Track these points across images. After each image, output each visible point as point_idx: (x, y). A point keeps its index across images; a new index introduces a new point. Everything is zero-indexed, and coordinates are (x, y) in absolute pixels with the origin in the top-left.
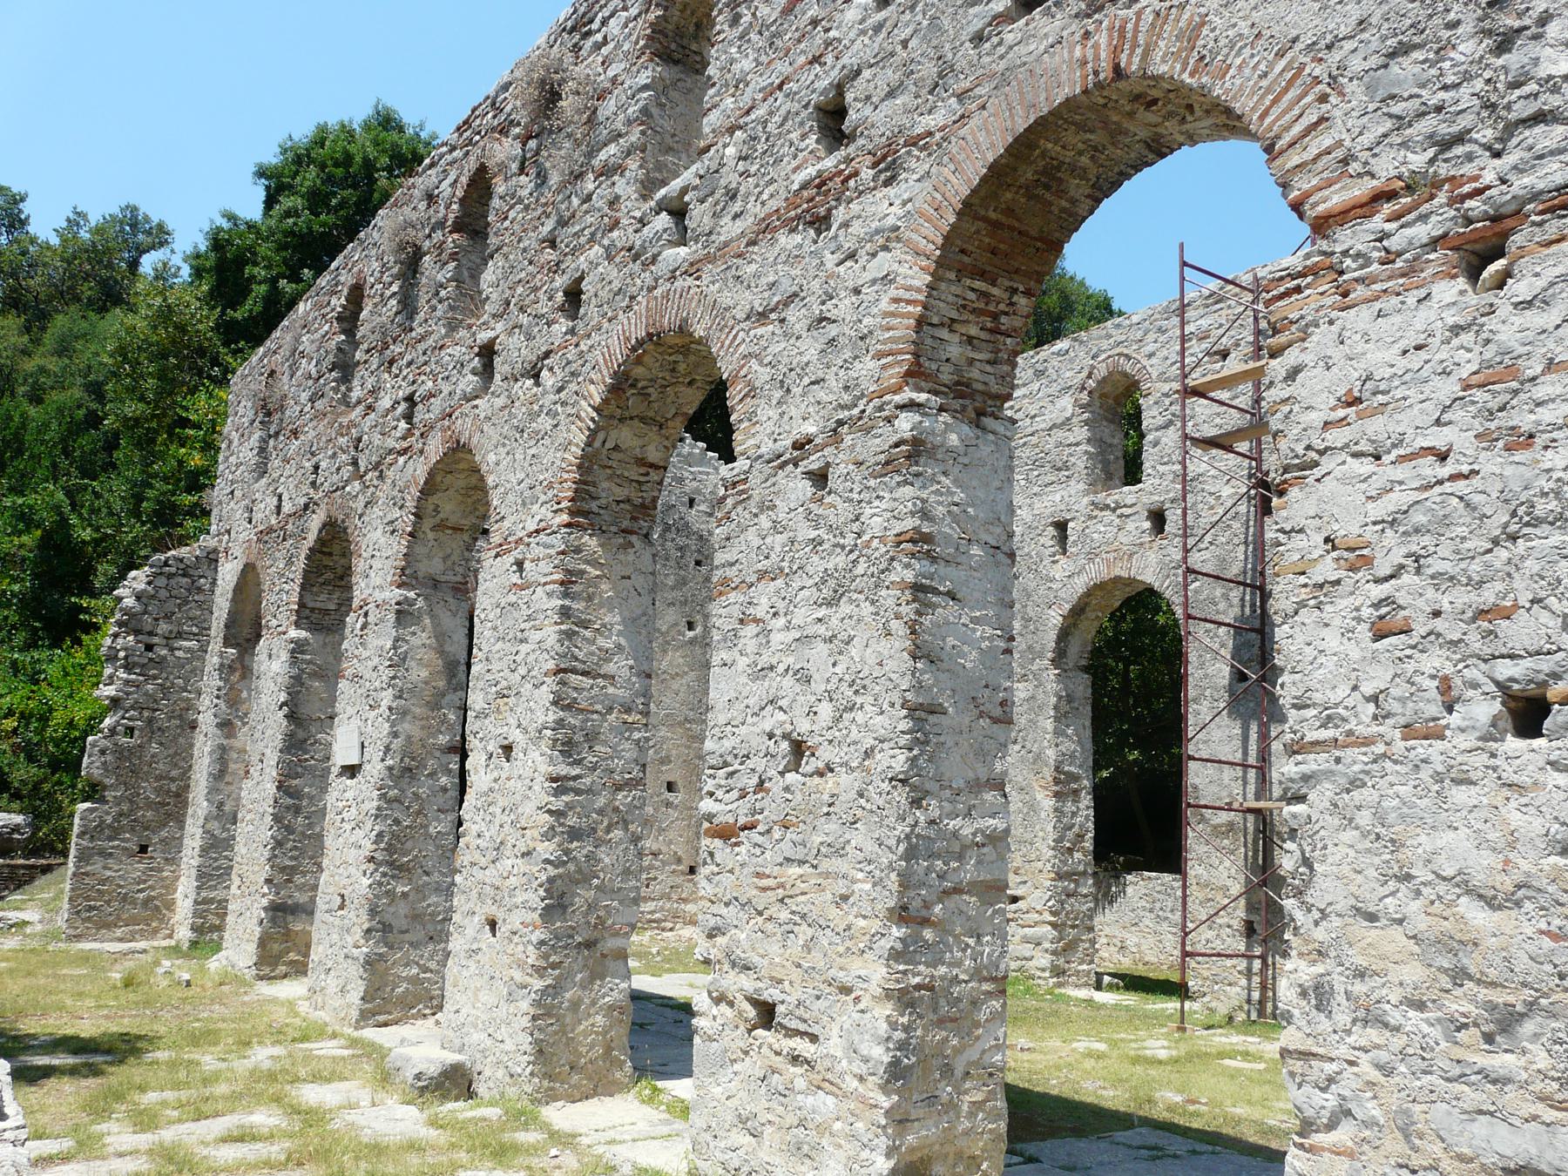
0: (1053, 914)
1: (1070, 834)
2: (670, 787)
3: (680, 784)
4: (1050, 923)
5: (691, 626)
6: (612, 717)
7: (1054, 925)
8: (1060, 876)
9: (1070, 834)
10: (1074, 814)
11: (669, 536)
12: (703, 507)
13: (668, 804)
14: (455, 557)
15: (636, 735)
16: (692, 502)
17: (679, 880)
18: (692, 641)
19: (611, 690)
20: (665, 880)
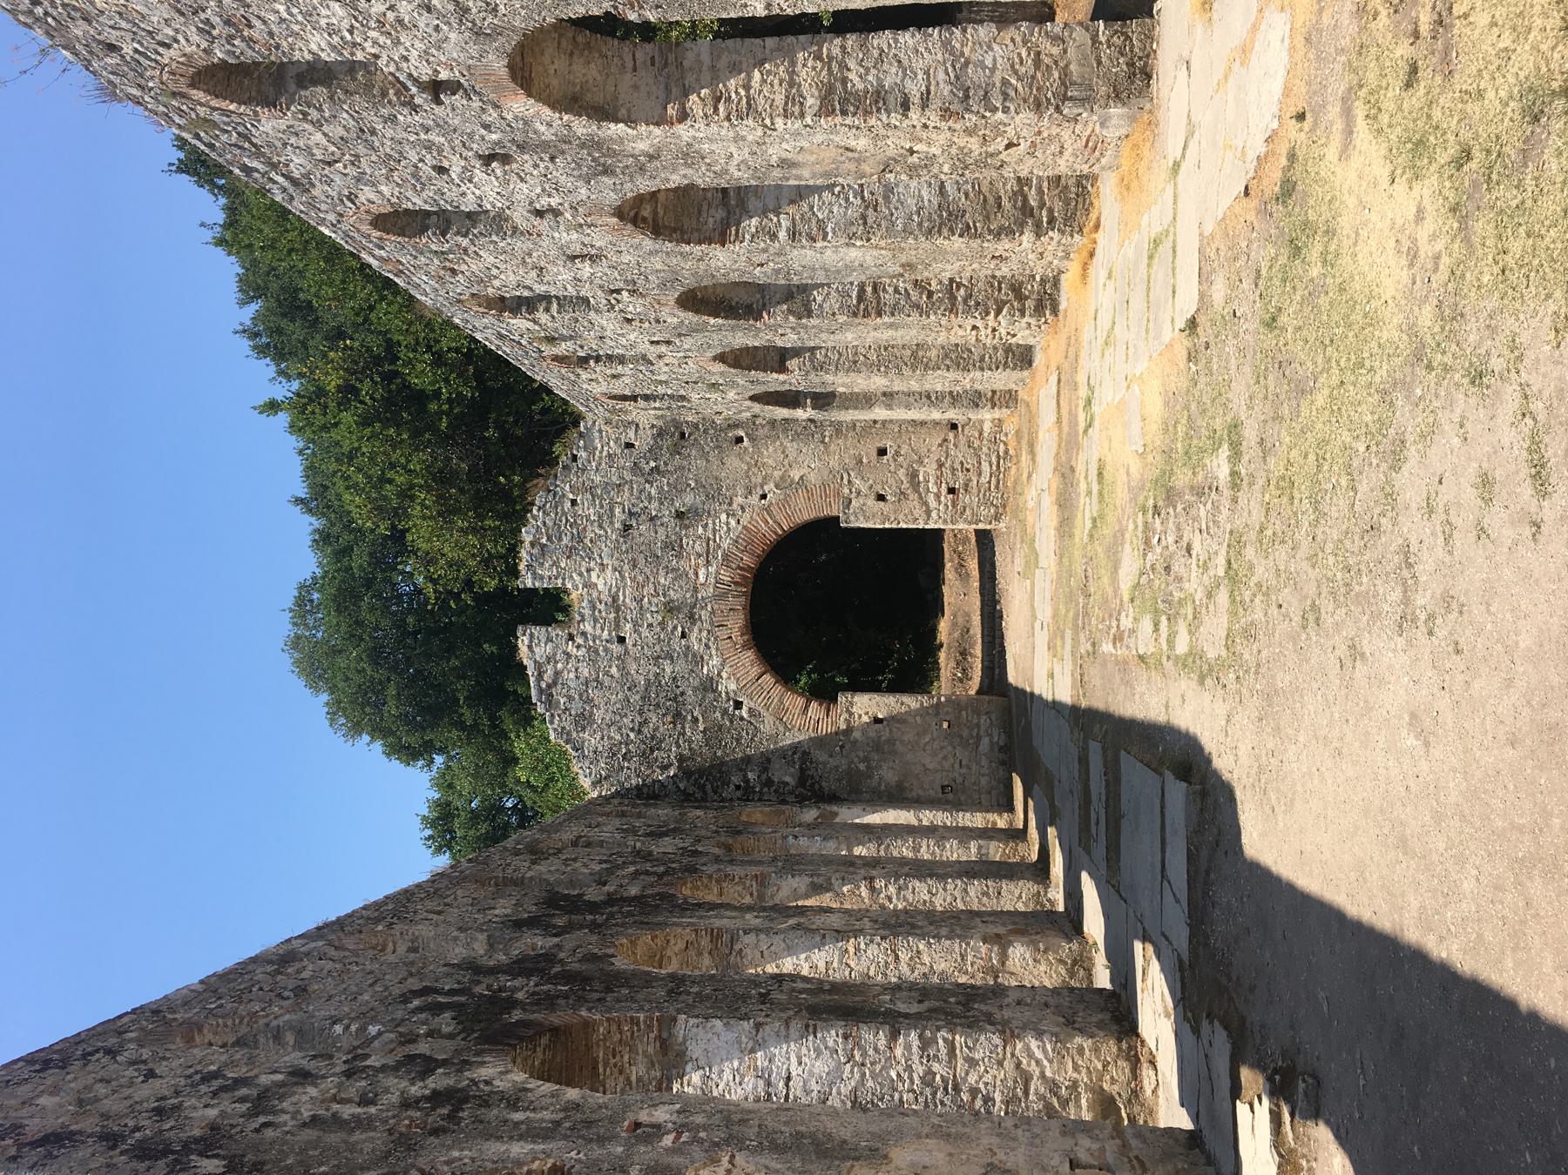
0: (988, 314)
1: (914, 295)
2: (882, 452)
3: (881, 445)
4: (997, 315)
5: (739, 440)
6: (852, 964)
7: (998, 312)
8: (953, 309)
9: (914, 295)
10: (896, 291)
11: (662, 468)
12: (631, 434)
13: (897, 453)
14: (740, 888)
15: (863, 946)
16: (629, 446)
17: (962, 440)
18: (752, 439)
19: (835, 965)
20: (959, 454)
